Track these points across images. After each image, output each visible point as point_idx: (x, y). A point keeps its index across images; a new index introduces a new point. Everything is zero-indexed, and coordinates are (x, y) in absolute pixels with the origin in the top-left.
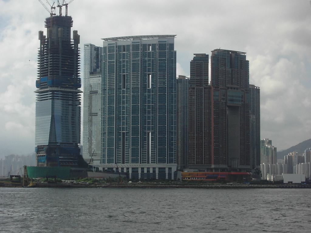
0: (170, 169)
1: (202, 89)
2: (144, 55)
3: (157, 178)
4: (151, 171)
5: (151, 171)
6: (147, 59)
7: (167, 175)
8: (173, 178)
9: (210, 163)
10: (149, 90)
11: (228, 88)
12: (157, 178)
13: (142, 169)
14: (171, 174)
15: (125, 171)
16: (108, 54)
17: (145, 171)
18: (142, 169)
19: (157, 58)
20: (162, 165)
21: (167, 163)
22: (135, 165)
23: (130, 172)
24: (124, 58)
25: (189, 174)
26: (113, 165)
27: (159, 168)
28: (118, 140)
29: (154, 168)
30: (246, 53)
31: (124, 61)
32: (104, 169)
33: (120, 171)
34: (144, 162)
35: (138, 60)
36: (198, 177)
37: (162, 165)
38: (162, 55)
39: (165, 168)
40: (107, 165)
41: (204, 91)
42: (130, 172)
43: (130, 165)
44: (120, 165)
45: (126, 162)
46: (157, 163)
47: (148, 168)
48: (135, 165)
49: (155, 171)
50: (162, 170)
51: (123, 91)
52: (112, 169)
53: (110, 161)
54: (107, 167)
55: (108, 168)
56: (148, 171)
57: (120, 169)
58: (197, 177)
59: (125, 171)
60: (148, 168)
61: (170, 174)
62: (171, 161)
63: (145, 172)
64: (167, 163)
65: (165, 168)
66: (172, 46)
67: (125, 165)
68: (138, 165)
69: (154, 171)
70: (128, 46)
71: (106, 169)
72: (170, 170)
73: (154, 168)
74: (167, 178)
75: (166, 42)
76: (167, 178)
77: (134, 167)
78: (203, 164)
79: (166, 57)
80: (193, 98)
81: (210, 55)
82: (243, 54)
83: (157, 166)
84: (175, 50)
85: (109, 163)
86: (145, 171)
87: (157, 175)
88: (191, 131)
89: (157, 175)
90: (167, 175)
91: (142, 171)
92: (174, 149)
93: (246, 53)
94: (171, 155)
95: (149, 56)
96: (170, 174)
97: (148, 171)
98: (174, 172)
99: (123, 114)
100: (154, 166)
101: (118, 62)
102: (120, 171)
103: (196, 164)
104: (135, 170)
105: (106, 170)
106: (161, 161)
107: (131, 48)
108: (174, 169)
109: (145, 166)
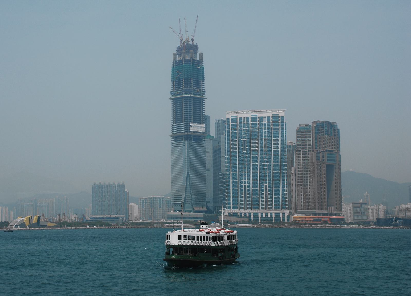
0: (284, 214)
1: (307, 152)
2: (261, 125)
3: (274, 221)
4: (269, 215)
5: (269, 215)
6: (263, 128)
7: (281, 219)
8: (286, 221)
10: (265, 153)
11: (326, 151)
12: (274, 221)
13: (262, 214)
14: (285, 218)
15: (248, 215)
16: (231, 124)
17: (264, 215)
18: (262, 214)
19: (271, 127)
21: (281, 209)
23: (252, 216)
25: (299, 217)
26: (238, 211)
27: (275, 213)
29: (271, 214)
30: (337, 123)
31: (244, 130)
32: (229, 213)
33: (243, 215)
34: (263, 209)
35: (255, 129)
36: (306, 220)
38: (276, 125)
39: (279, 213)
41: (309, 153)
42: (252, 216)
43: (252, 211)
44: (243, 211)
45: (248, 209)
46: (273, 209)
47: (266, 214)
49: (272, 215)
50: (277, 215)
52: (237, 213)
54: (231, 213)
55: (233, 213)
56: (267, 215)
58: (305, 220)
59: (248, 215)
60: (266, 214)
61: (284, 218)
62: (284, 208)
63: (264, 216)
64: (281, 209)
65: (279, 213)
67: (247, 211)
69: (271, 215)
70: (248, 118)
72: (284, 215)
74: (281, 220)
75: (278, 115)
76: (281, 220)
77: (255, 212)
78: (309, 210)
79: (279, 127)
80: (300, 158)
81: (311, 124)
82: (335, 124)
83: (274, 211)
85: (234, 209)
86: (264, 215)
87: (274, 218)
88: (299, 184)
89: (274, 218)
90: (281, 219)
91: (262, 215)
92: (286, 198)
93: (337, 123)
94: (284, 203)
95: (265, 126)
96: (284, 218)
97: (267, 215)
98: (287, 216)
99: (245, 171)
101: (240, 131)
102: (243, 215)
103: (304, 210)
104: (256, 215)
105: (232, 215)
106: (277, 207)
107: (250, 119)
108: (286, 215)
109: (264, 211)
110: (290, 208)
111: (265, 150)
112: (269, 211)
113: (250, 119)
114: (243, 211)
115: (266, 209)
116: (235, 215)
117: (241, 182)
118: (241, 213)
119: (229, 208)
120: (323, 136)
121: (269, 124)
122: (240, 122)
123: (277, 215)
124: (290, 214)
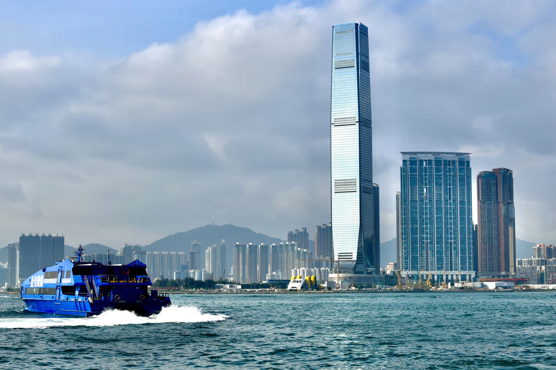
0: (470, 275)
6: (448, 174)
9: (500, 270)
13: (447, 276)
17: (450, 278)
18: (447, 276)
22: (439, 272)
24: (426, 172)
27: (462, 275)
31: (426, 175)
37: (463, 273)
40: (411, 273)
47: (452, 275)
48: (439, 272)
51: (426, 203)
53: (414, 268)
56: (452, 278)
57: (425, 276)
60: (452, 275)
62: (470, 269)
65: (466, 275)
66: (468, 162)
67: (430, 273)
71: (410, 276)
73: (457, 275)
84: (470, 166)
86: (450, 278)
91: (447, 278)
94: (470, 263)
97: (452, 278)
100: (457, 273)
108: (473, 276)
109: (449, 273)
110: (476, 269)
111: (450, 200)
113: (434, 163)
115: (451, 270)
117: (422, 238)
119: (406, 268)
120: (498, 185)
121: (454, 170)
122: (445, 165)
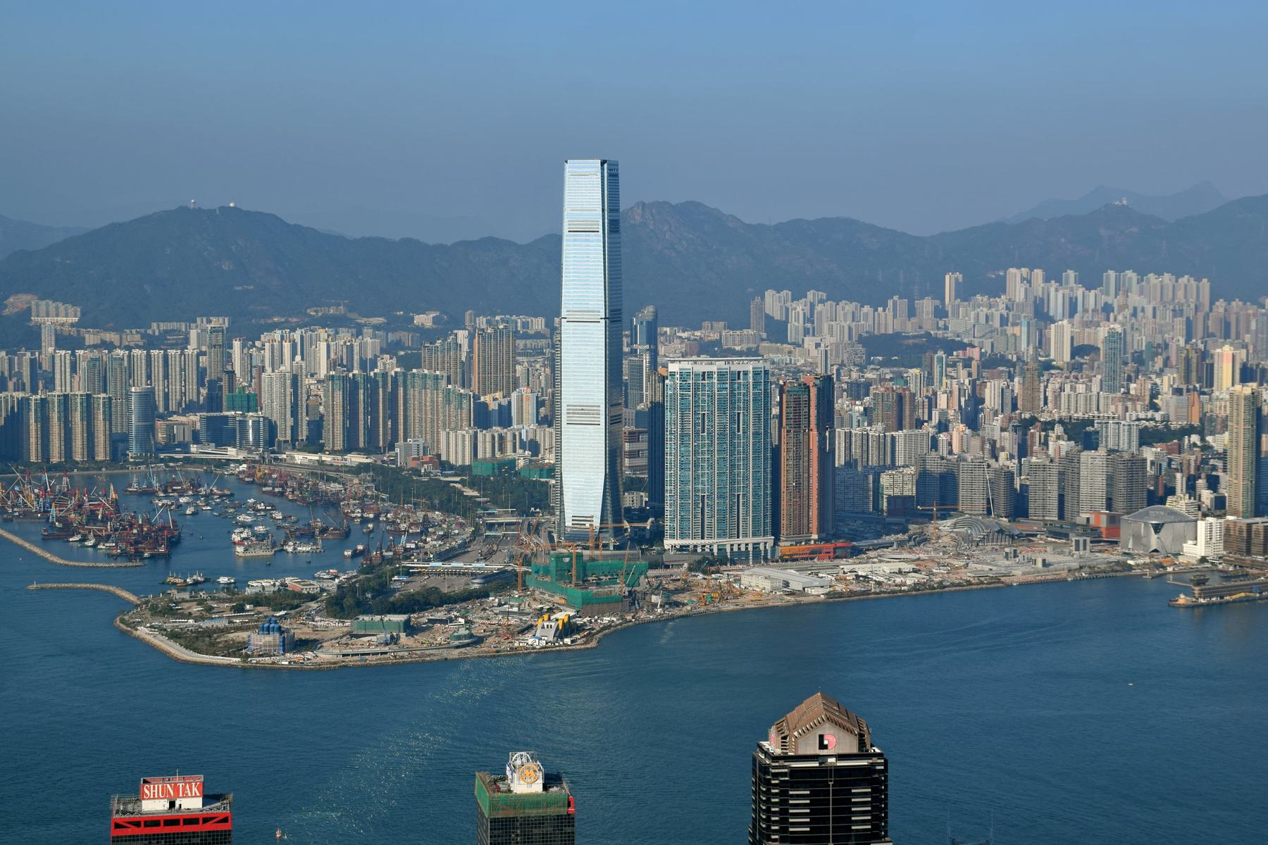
4: (743, 549)
5: (743, 549)
9: (809, 532)
17: (735, 549)
20: (756, 540)
28: (696, 504)
37: (756, 540)
40: (678, 542)
42: (715, 551)
44: (699, 542)
50: (756, 546)
53: (683, 536)
61: (766, 551)
68: (727, 542)
83: (751, 540)
86: (735, 549)
96: (766, 551)
101: (695, 395)
109: (735, 541)
112: (742, 540)
114: (699, 542)
116: (683, 548)
118: (695, 546)
119: (672, 536)
123: (756, 546)
124: (776, 544)
